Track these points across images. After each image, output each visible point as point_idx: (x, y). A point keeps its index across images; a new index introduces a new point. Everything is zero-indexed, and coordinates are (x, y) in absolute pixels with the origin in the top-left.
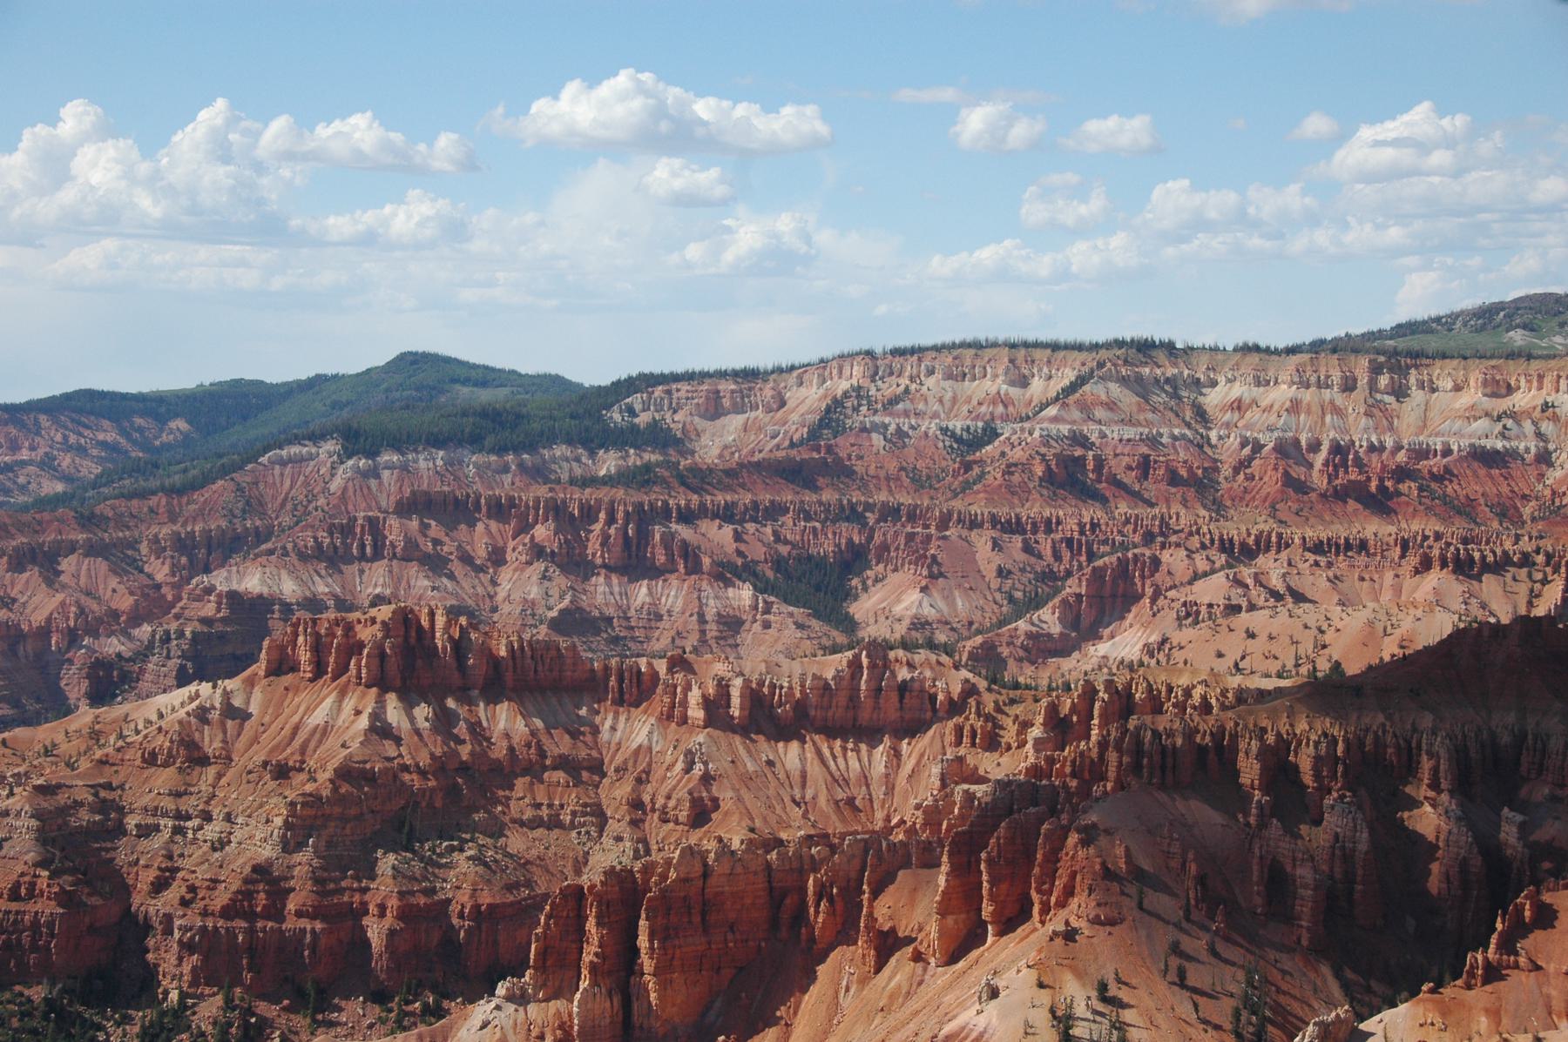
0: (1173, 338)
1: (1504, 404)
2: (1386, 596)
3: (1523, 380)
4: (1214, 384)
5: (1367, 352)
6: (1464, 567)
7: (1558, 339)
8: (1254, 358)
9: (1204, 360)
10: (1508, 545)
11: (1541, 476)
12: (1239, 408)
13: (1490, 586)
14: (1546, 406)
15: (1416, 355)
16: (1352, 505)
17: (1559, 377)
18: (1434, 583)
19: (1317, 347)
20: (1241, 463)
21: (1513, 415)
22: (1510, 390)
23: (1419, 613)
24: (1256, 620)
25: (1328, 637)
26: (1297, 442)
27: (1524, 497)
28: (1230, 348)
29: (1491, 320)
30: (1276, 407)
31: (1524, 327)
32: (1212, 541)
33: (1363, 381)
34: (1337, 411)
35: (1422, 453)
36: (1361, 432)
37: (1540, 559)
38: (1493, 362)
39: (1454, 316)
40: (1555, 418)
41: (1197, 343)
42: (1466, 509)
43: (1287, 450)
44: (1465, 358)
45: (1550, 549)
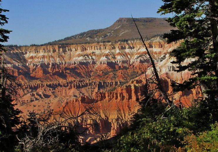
0: (17, 45)
1: (85, 52)
2: (64, 95)
3: (88, 48)
4: (26, 53)
5: (57, 44)
6: (78, 87)
7: (96, 39)
8: (34, 47)
9: (24, 48)
10: (88, 82)
11: (93, 67)
12: (32, 58)
13: (83, 90)
14: (93, 53)
15: (67, 44)
16: (56, 76)
17: (95, 47)
18: (73, 91)
19: (50, 44)
20: (33, 69)
21: (88, 56)
22: (86, 50)
23: (68, 98)
24: (36, 102)
25: (50, 105)
26: (45, 64)
27: (91, 71)
28: (29, 45)
29: (83, 36)
30: (40, 57)
31: (89, 37)
32: (28, 86)
33: (57, 50)
34: (52, 57)
35: (70, 64)
36: (58, 60)
37: (93, 84)
38: (82, 45)
39: (76, 36)
40: (95, 55)
41: (22, 45)
42: (79, 75)
43: (44, 67)
44: (77, 44)
45: (94, 81)
